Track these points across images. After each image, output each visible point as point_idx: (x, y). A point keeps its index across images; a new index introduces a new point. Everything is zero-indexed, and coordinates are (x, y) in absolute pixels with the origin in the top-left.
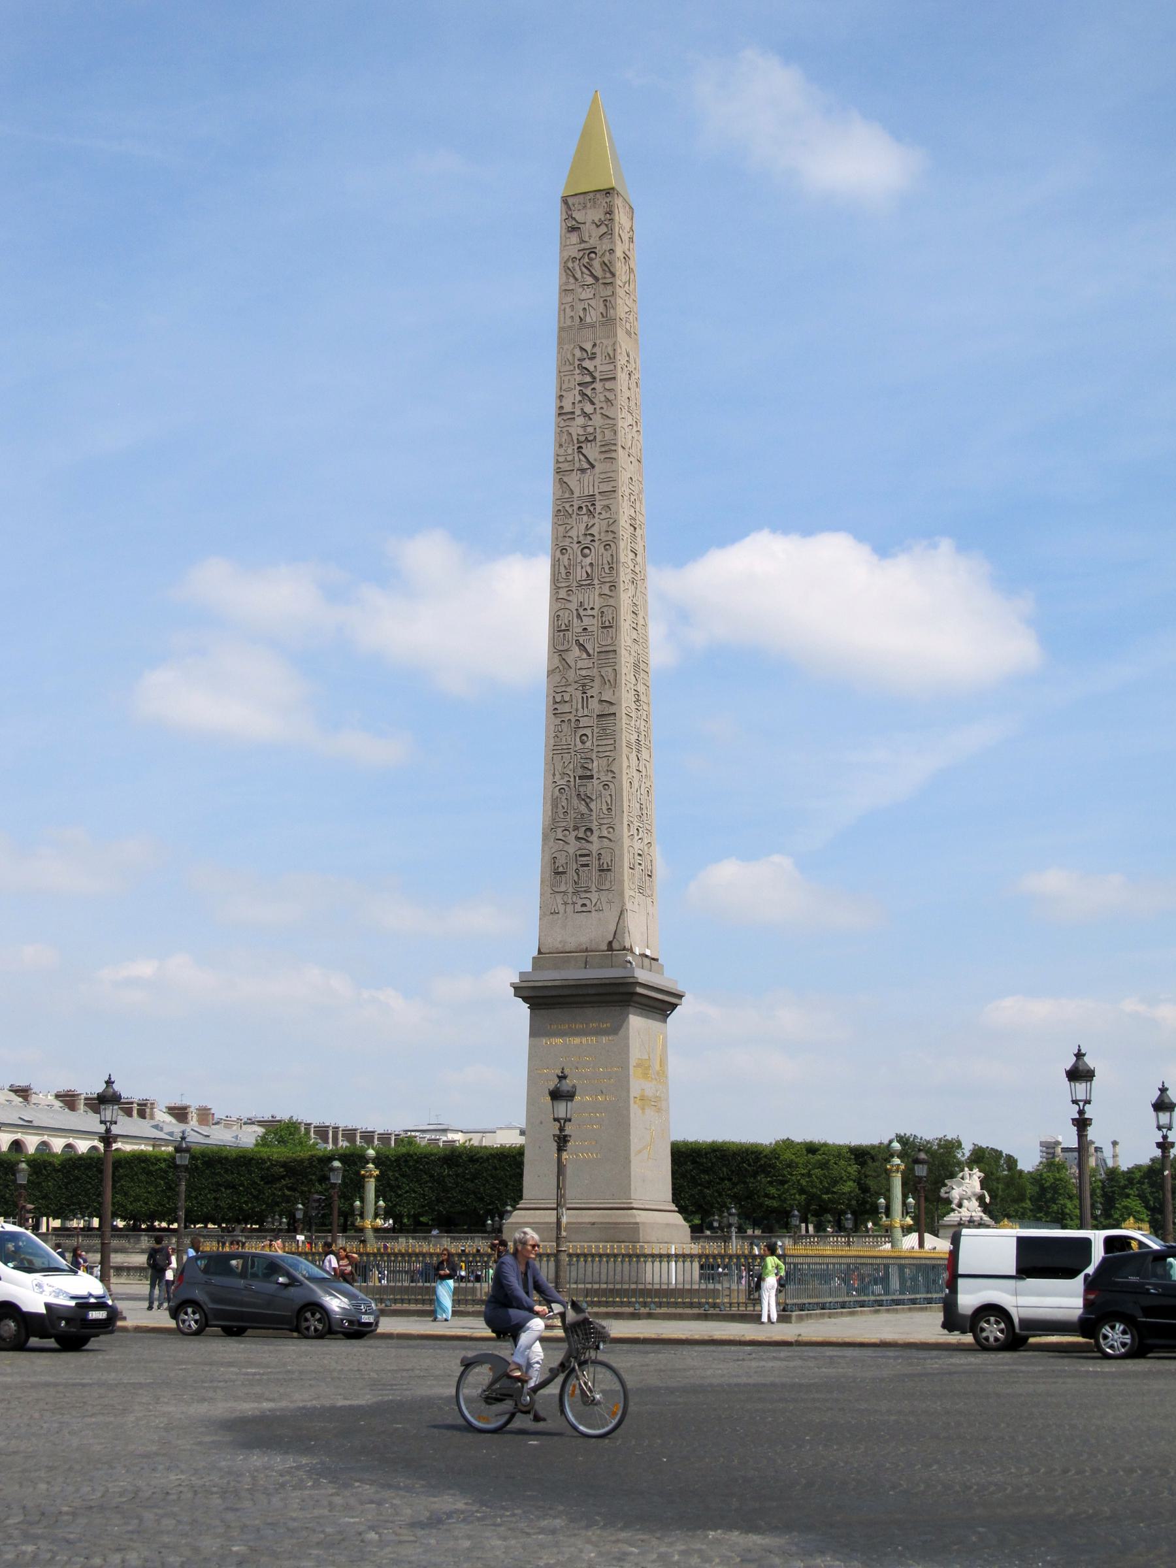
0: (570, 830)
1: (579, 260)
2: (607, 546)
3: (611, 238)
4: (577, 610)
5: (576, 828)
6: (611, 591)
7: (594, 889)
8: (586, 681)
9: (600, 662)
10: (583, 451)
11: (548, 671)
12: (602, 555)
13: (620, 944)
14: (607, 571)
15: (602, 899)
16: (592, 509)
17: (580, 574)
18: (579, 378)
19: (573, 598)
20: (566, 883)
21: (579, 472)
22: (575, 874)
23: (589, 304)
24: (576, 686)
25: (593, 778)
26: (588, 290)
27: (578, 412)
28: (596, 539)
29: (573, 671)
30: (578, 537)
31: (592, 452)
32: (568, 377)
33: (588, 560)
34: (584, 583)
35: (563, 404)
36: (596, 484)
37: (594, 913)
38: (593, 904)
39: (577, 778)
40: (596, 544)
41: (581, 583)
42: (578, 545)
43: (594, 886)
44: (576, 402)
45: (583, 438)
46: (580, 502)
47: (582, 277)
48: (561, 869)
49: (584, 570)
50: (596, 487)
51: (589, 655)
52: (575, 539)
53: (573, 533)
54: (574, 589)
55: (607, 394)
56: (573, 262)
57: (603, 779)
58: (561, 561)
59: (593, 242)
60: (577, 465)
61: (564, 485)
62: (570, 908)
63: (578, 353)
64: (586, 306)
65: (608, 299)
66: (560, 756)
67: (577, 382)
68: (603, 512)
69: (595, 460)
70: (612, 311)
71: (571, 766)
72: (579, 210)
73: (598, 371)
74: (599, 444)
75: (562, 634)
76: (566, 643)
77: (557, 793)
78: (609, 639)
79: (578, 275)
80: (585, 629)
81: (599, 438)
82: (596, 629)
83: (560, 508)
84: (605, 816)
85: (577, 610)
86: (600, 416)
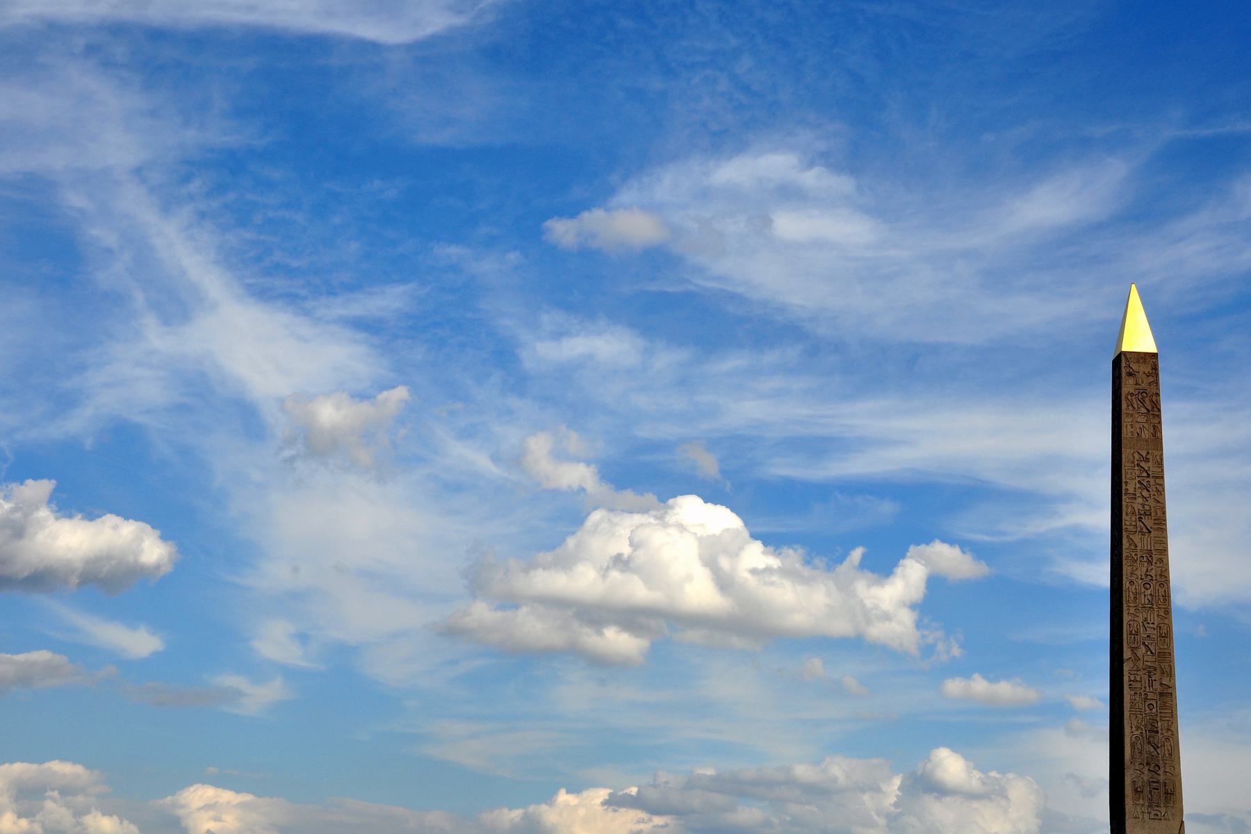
2: (1161, 585)
5: (1148, 764)
6: (1165, 614)
7: (1162, 805)
8: (1150, 670)
10: (1143, 520)
17: (1143, 600)
23: (1143, 427)
28: (1154, 579)
29: (1141, 662)
30: (1141, 576)
31: (1149, 522)
33: (1148, 592)
35: (1127, 487)
36: (1152, 543)
40: (1154, 582)
45: (1142, 512)
48: (1139, 789)
50: (1152, 546)
51: (1152, 653)
53: (1139, 573)
55: (1158, 487)
60: (1139, 529)
62: (1146, 816)
63: (1137, 456)
64: (1141, 427)
70: (1158, 433)
71: (1143, 724)
72: (1134, 363)
74: (1153, 518)
77: (1134, 739)
79: (1135, 406)
81: (1153, 514)
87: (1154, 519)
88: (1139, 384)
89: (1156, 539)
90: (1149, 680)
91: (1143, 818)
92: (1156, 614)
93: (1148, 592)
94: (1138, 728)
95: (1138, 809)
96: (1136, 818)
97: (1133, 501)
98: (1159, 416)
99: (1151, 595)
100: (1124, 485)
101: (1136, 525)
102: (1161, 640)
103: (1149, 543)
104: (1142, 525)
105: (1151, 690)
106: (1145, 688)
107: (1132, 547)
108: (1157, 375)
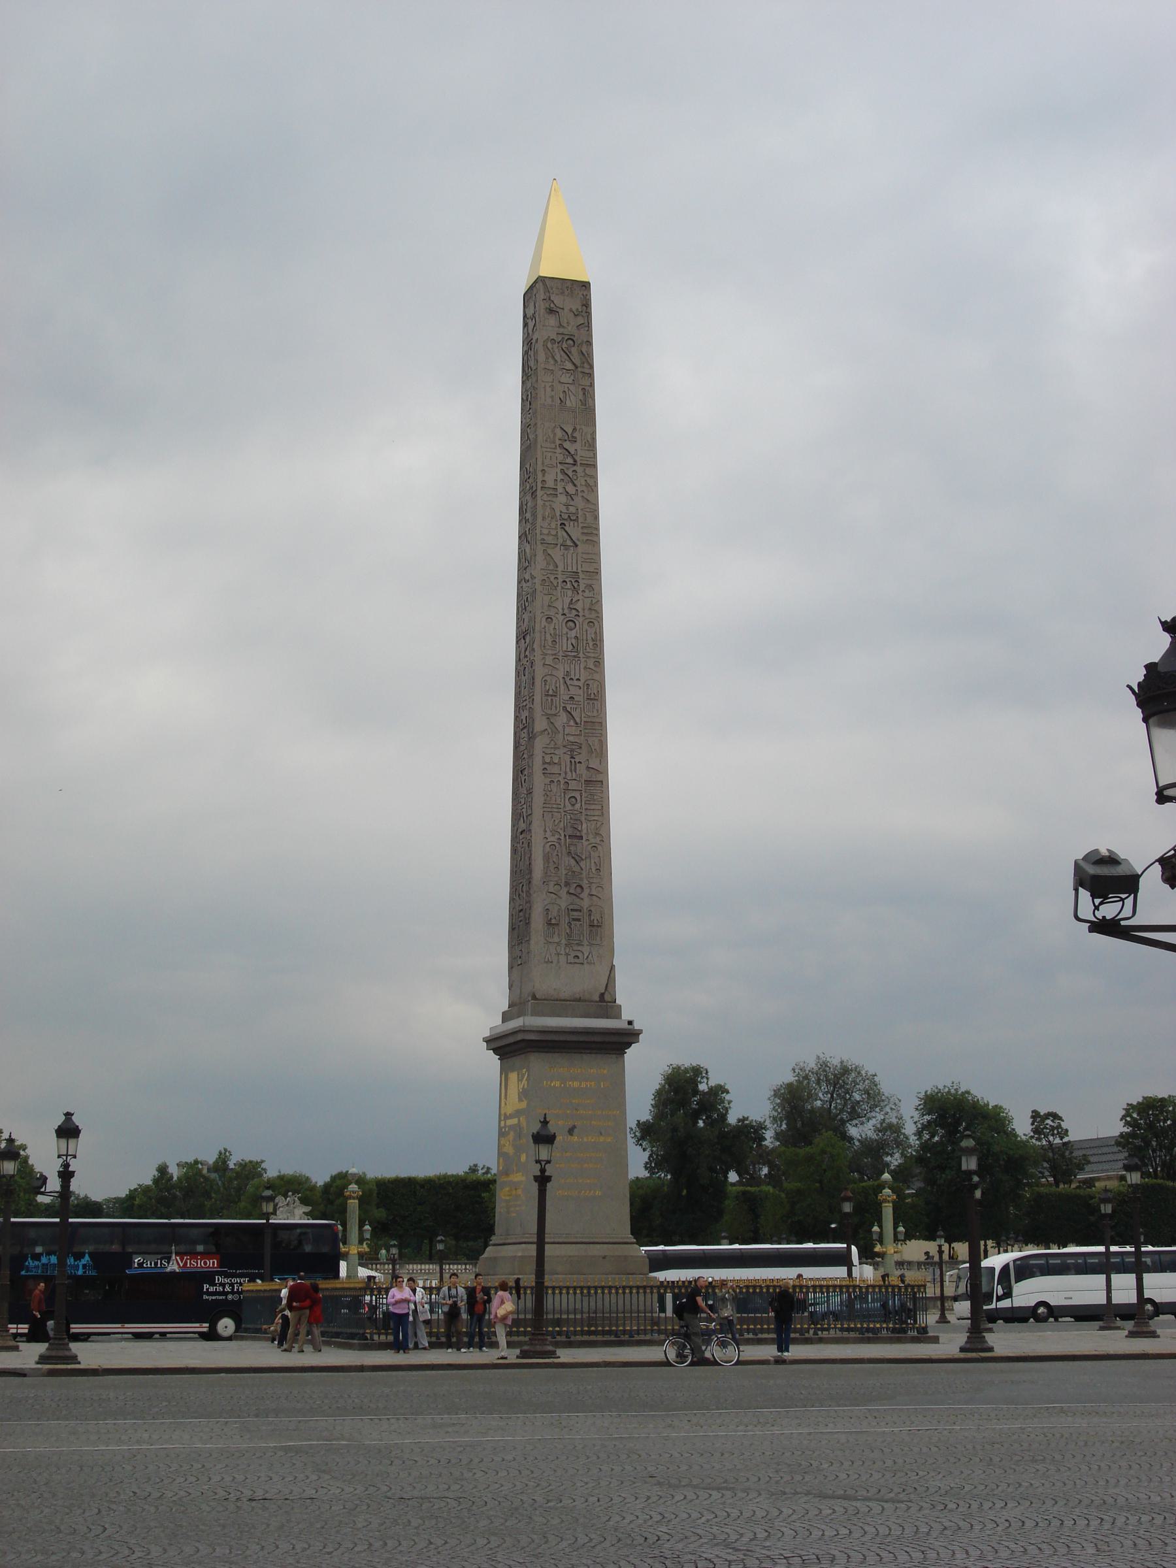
0: (563, 886)
1: (558, 343)
3: (588, 330)
4: (563, 678)
5: (567, 884)
6: (595, 666)
7: (585, 942)
8: (574, 747)
9: (587, 731)
10: (567, 528)
12: (587, 631)
14: (591, 647)
16: (576, 585)
17: (565, 645)
18: (560, 458)
19: (560, 666)
20: (559, 934)
21: (562, 547)
22: (567, 927)
24: (565, 750)
25: (582, 839)
26: (568, 375)
27: (560, 490)
28: (580, 614)
29: (561, 736)
30: (563, 609)
31: (575, 532)
32: (550, 454)
33: (573, 634)
34: (570, 654)
37: (586, 966)
38: (585, 957)
39: (567, 837)
40: (581, 619)
41: (567, 653)
42: (563, 617)
44: (559, 480)
45: (566, 517)
46: (565, 576)
47: (562, 361)
48: (553, 921)
49: (569, 642)
52: (561, 611)
54: (560, 658)
55: (588, 479)
56: (552, 344)
57: (592, 840)
58: (547, 628)
59: (570, 329)
60: (560, 541)
61: (548, 558)
62: (563, 959)
63: (559, 433)
65: (586, 388)
66: (550, 814)
67: (558, 462)
68: (587, 591)
69: (578, 540)
71: (562, 825)
72: (557, 294)
73: (578, 456)
74: (581, 525)
75: (549, 698)
76: (554, 708)
77: (548, 849)
78: (595, 711)
79: (558, 358)
80: (571, 698)
82: (582, 700)
83: (545, 578)
84: (595, 876)
85: (563, 678)
86: (580, 498)
87: (582, 528)
88: (563, 327)
89: (584, 556)
90: (571, 761)
91: (558, 962)
92: (582, 667)
93: (573, 634)
94: (554, 832)
96: (547, 962)
97: (554, 499)
98: (591, 375)
99: (576, 637)
100: (540, 475)
101: (556, 535)
102: (588, 703)
103: (574, 561)
104: (565, 534)
106: (566, 773)
107: (551, 567)
108: (589, 314)
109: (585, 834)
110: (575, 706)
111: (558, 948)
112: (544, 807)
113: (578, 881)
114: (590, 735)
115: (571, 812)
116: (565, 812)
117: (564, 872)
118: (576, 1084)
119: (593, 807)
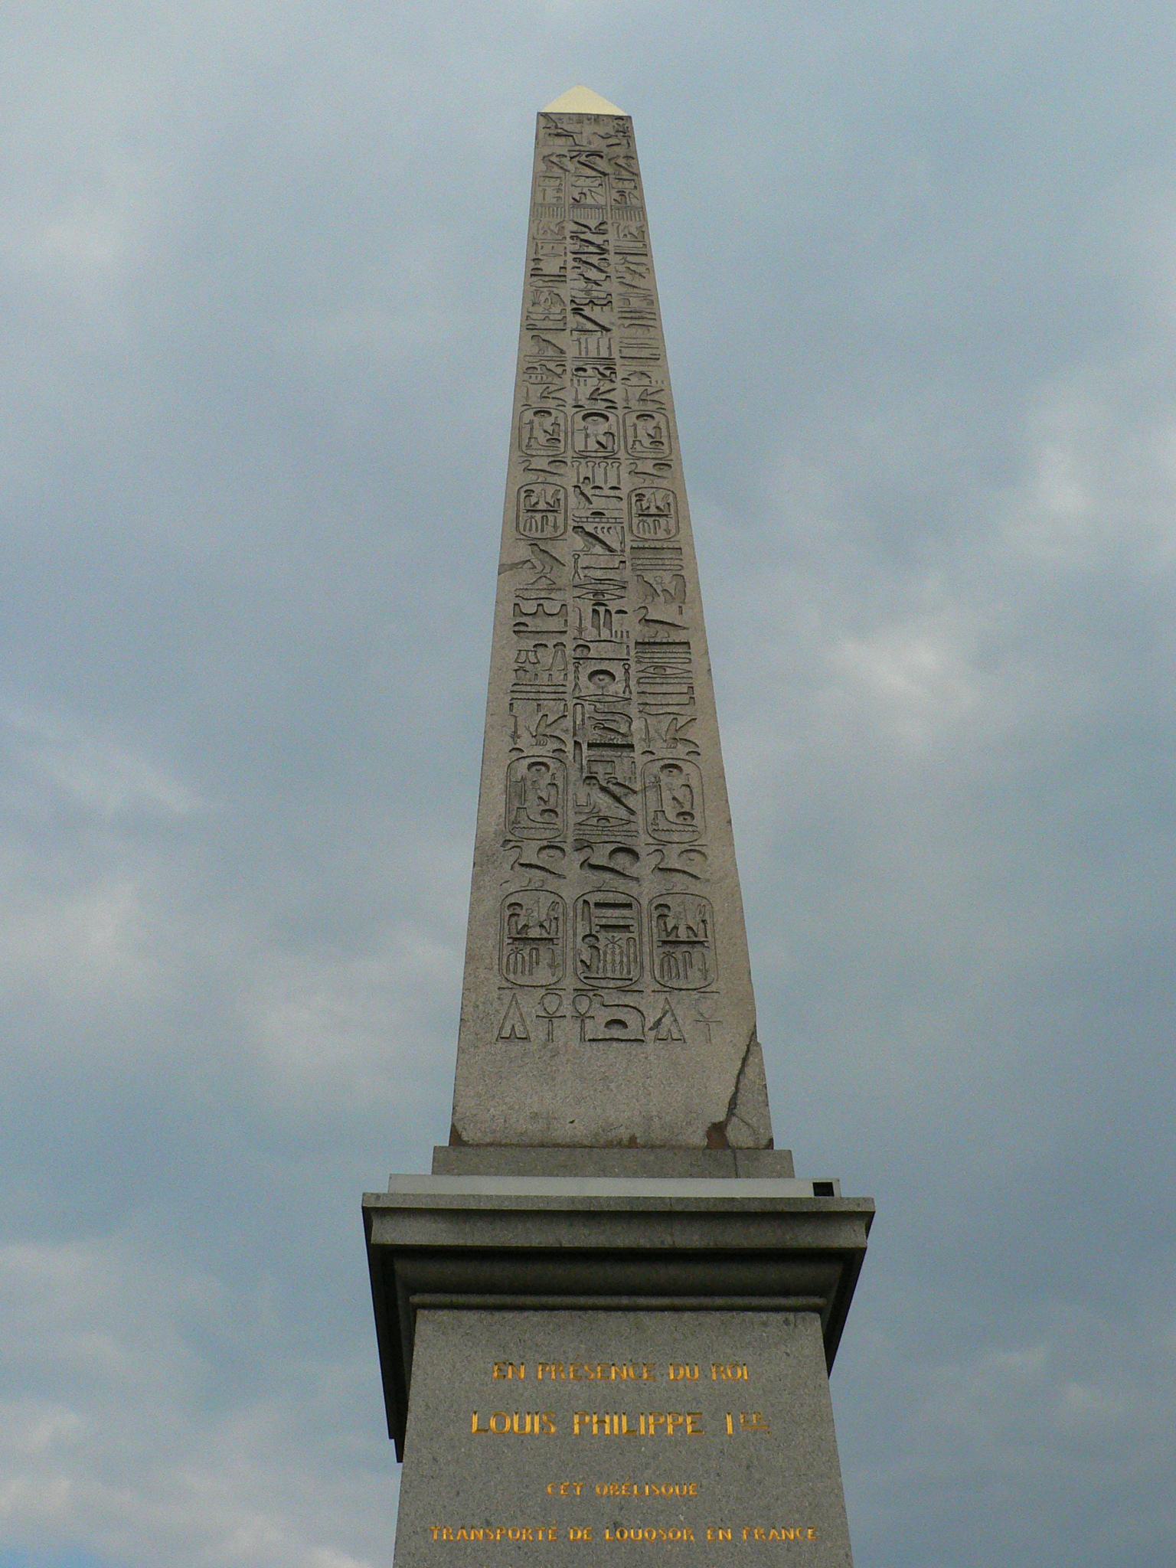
0: (568, 848)
7: (648, 983)
11: (501, 566)
13: (755, 1132)
15: (679, 1012)
37: (650, 1046)
39: (585, 747)
43: (647, 976)
62: (567, 1031)
75: (538, 516)
95: (529, 1004)
105: (605, 634)
109: (641, 739)
110: (608, 525)
111: (551, 1004)
112: (512, 692)
113: (618, 839)
114: (646, 567)
115: (593, 698)
116: (578, 698)
117: (573, 819)
118: (617, 1424)
119: (664, 689)
